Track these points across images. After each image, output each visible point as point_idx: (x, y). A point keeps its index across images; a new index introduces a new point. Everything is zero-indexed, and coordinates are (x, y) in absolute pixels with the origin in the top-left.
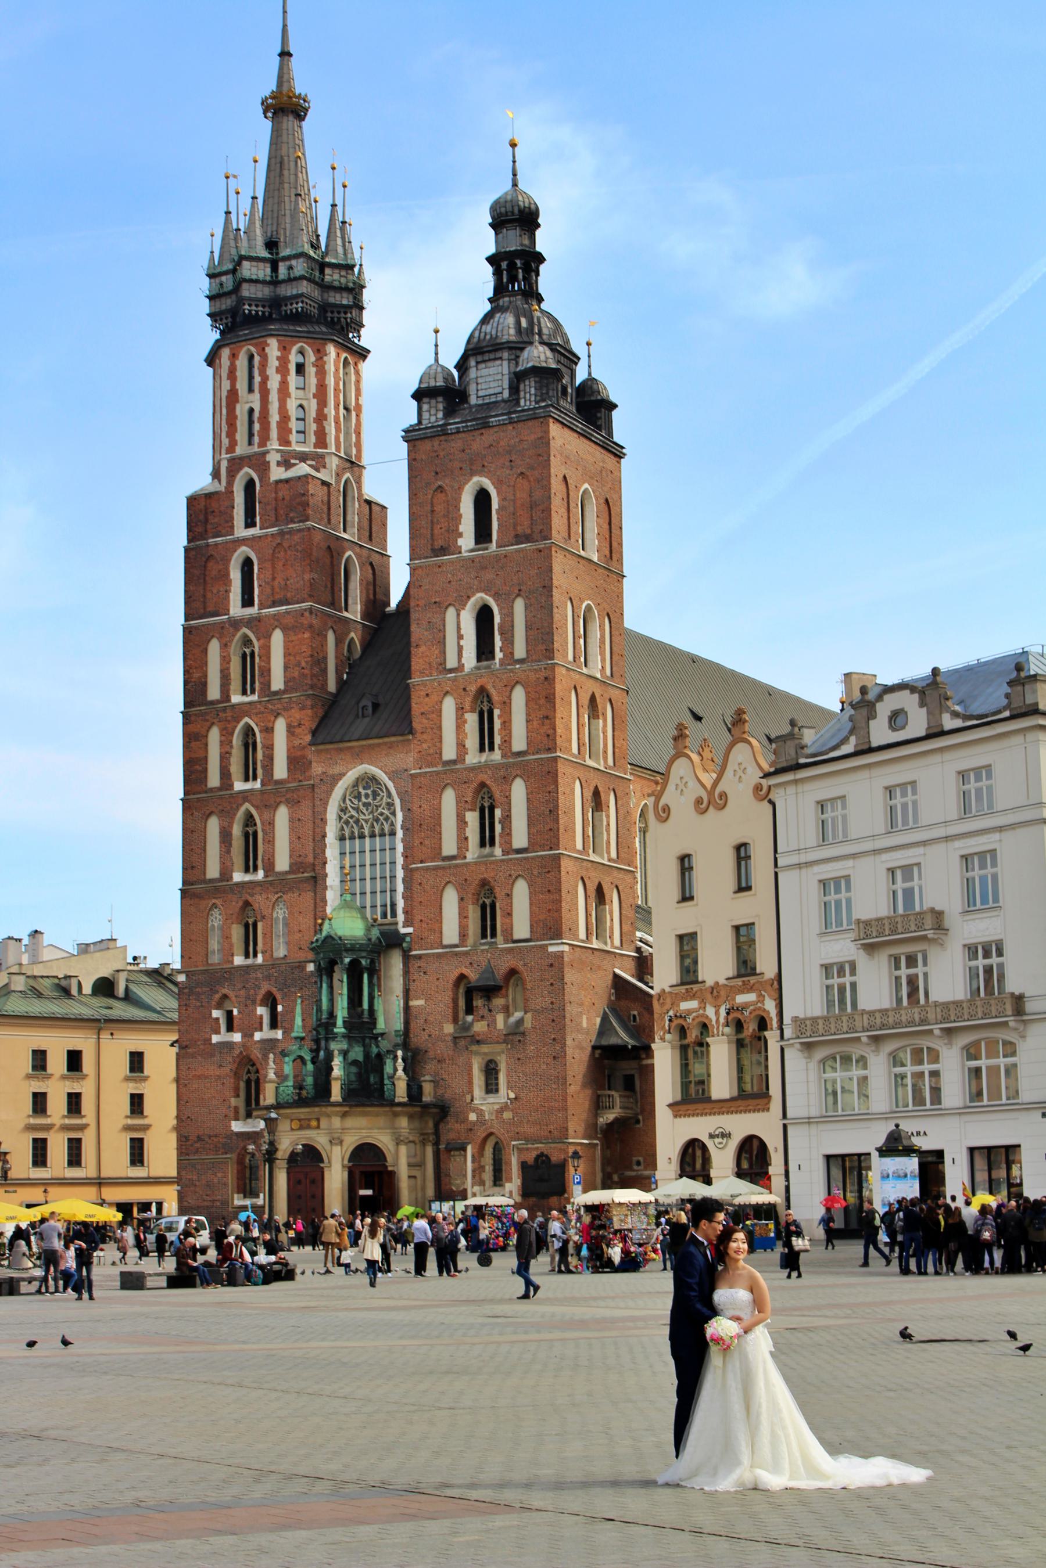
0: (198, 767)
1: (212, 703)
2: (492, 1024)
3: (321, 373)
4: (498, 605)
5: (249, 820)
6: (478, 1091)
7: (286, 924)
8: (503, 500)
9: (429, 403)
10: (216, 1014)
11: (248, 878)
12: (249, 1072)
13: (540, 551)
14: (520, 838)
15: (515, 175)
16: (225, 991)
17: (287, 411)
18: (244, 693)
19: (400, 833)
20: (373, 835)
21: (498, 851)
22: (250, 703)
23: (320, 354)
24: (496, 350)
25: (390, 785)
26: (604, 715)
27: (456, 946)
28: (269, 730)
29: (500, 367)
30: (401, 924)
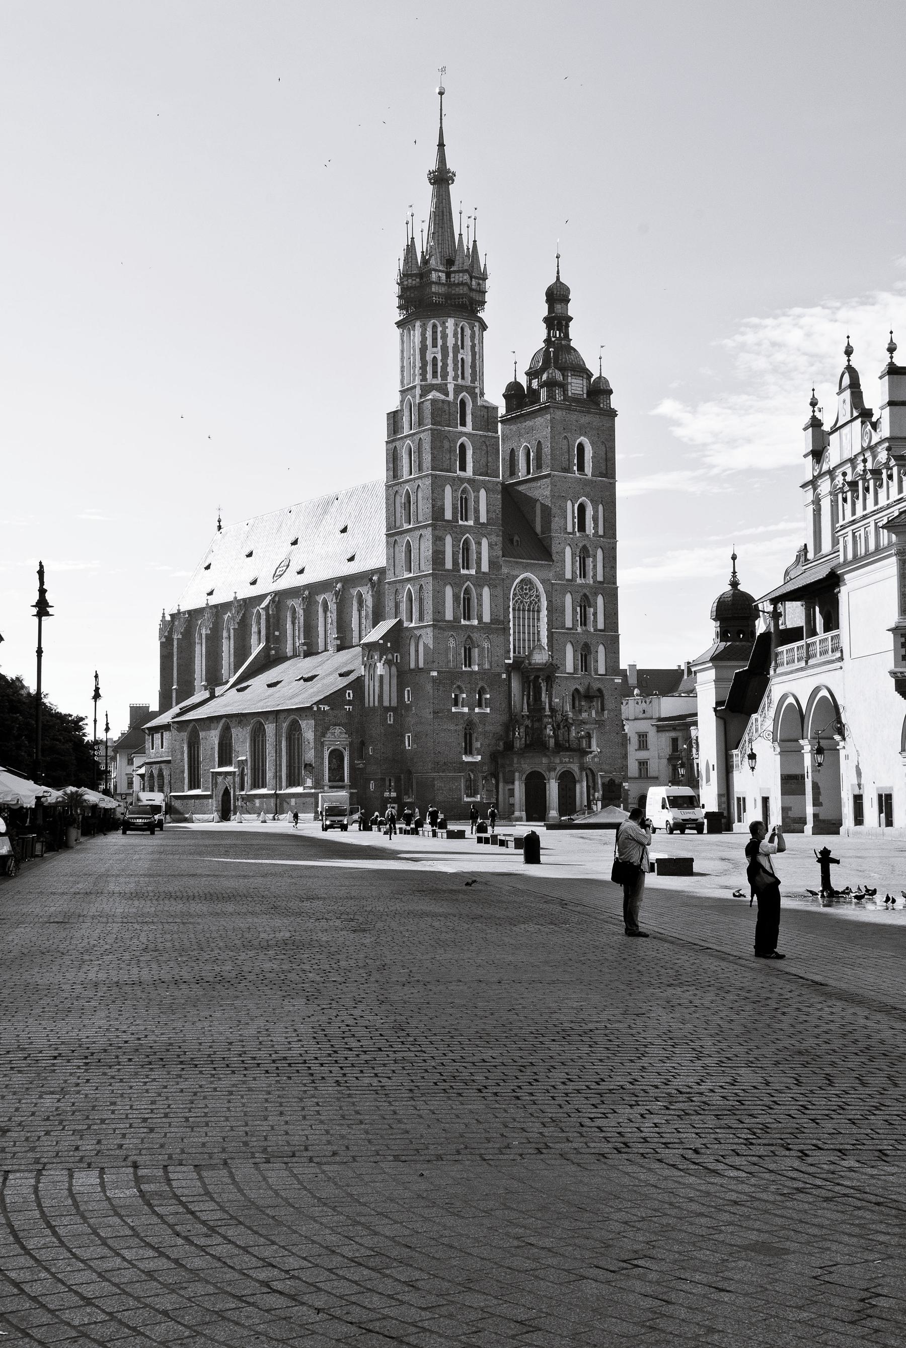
1: (448, 521)
2: (590, 715)
5: (467, 591)
7: (488, 651)
8: (594, 453)
11: (467, 623)
12: (466, 729)
13: (611, 483)
15: (558, 273)
16: (459, 683)
18: (462, 519)
20: (529, 610)
21: (592, 630)
22: (471, 526)
24: (580, 372)
27: (573, 674)
28: (479, 544)
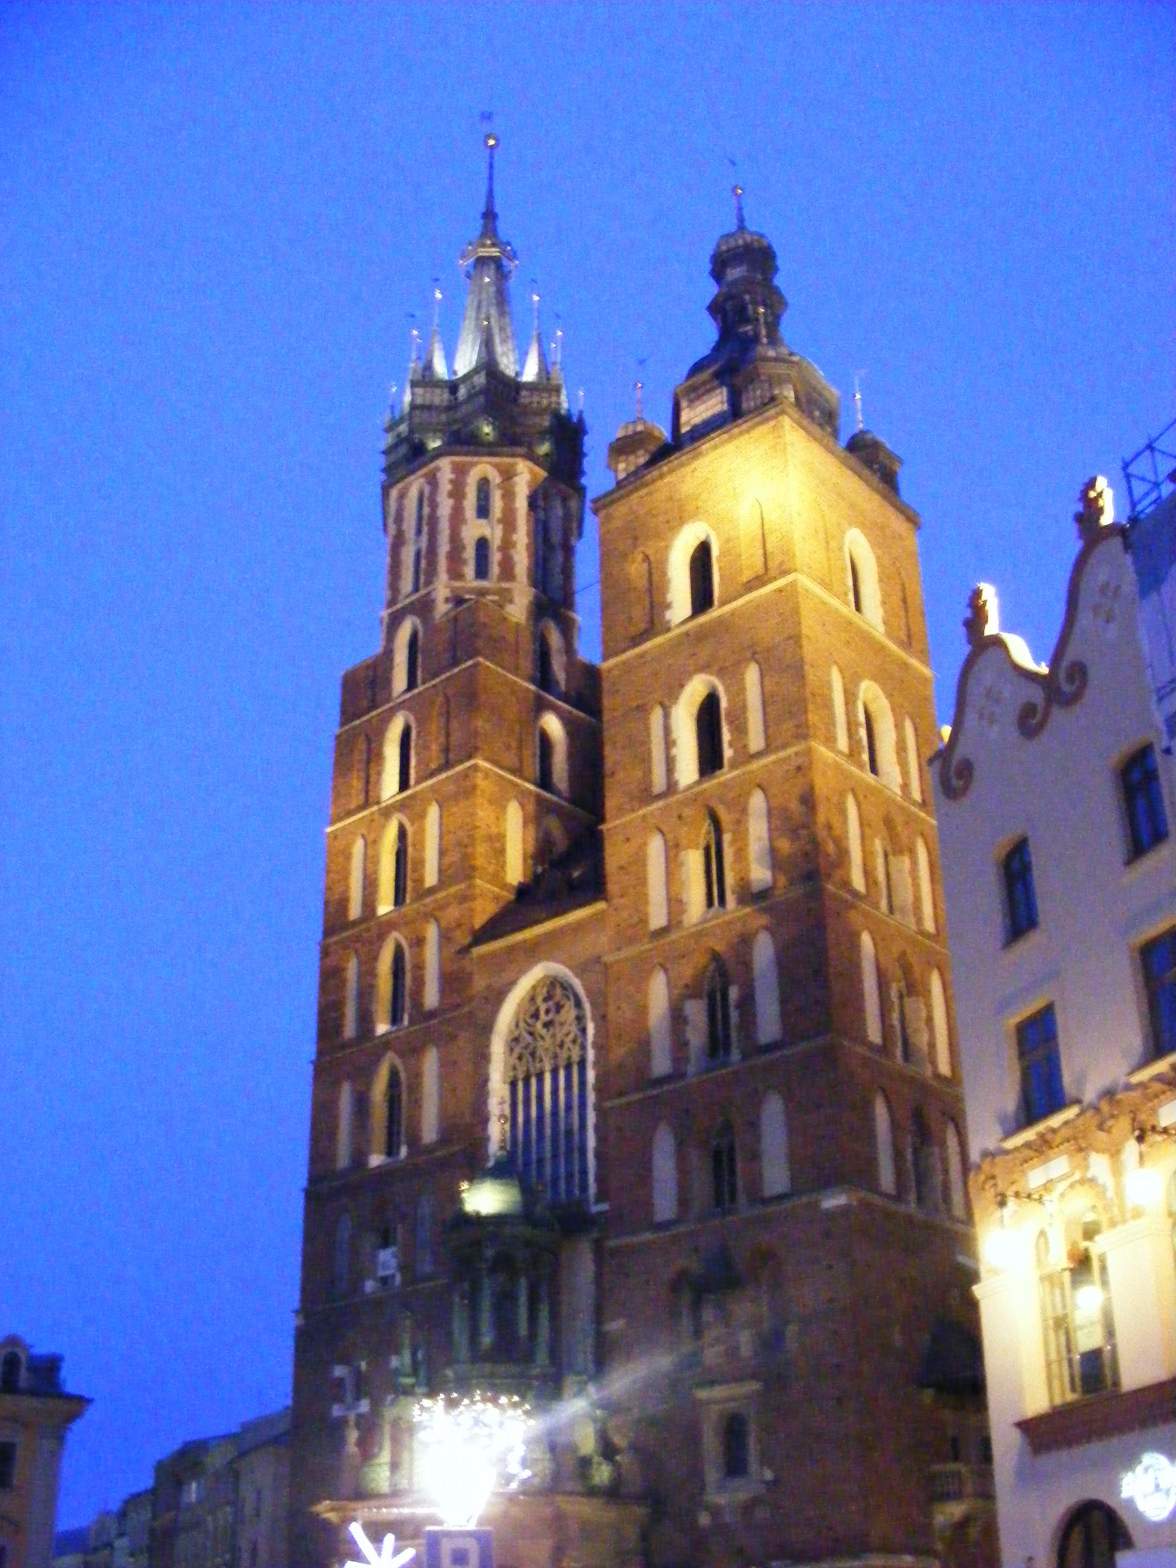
0: (333, 1014)
1: (355, 924)
3: (509, 496)
4: (724, 684)
6: (712, 1475)
9: (626, 461)
10: (339, 1371)
14: (769, 1025)
17: (461, 540)
19: (591, 1055)
23: (508, 475)
25: (577, 983)
26: (912, 852)
28: (419, 942)
29: (719, 398)
30: (592, 1198)
